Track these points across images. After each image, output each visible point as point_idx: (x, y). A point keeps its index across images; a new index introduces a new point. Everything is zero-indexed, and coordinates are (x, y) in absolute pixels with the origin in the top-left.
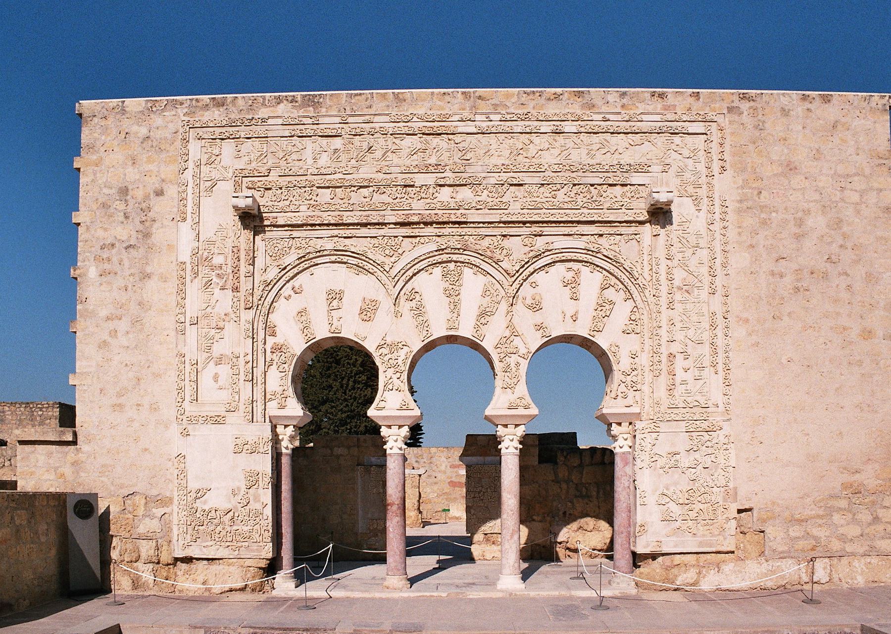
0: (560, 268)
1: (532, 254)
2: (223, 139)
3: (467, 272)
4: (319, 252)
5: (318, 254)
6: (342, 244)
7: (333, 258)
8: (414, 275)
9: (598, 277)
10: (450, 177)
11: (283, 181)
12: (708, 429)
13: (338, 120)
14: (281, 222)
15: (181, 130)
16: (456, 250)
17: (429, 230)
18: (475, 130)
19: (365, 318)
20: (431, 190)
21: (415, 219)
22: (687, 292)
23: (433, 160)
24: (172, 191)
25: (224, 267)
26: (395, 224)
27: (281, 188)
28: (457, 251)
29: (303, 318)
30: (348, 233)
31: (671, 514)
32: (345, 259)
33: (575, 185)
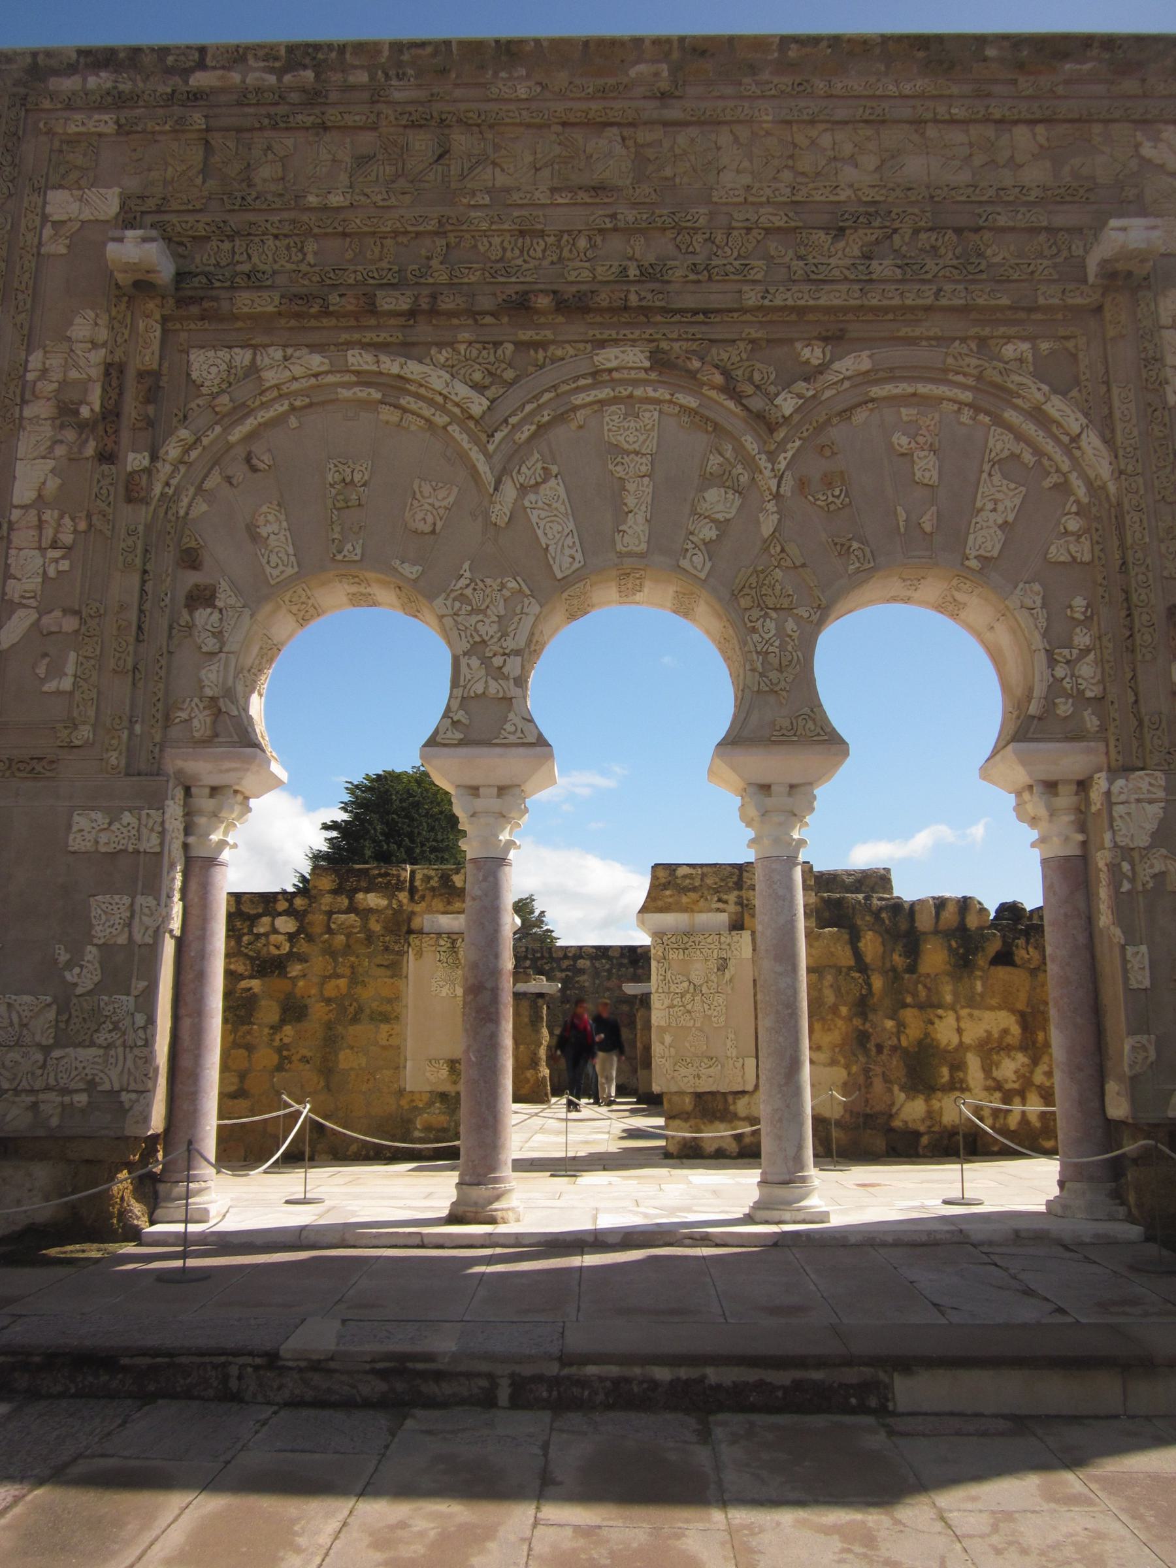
4: (316, 376)
10: (628, 215)
20: (582, 243)
27: (231, 238)
29: (269, 529)
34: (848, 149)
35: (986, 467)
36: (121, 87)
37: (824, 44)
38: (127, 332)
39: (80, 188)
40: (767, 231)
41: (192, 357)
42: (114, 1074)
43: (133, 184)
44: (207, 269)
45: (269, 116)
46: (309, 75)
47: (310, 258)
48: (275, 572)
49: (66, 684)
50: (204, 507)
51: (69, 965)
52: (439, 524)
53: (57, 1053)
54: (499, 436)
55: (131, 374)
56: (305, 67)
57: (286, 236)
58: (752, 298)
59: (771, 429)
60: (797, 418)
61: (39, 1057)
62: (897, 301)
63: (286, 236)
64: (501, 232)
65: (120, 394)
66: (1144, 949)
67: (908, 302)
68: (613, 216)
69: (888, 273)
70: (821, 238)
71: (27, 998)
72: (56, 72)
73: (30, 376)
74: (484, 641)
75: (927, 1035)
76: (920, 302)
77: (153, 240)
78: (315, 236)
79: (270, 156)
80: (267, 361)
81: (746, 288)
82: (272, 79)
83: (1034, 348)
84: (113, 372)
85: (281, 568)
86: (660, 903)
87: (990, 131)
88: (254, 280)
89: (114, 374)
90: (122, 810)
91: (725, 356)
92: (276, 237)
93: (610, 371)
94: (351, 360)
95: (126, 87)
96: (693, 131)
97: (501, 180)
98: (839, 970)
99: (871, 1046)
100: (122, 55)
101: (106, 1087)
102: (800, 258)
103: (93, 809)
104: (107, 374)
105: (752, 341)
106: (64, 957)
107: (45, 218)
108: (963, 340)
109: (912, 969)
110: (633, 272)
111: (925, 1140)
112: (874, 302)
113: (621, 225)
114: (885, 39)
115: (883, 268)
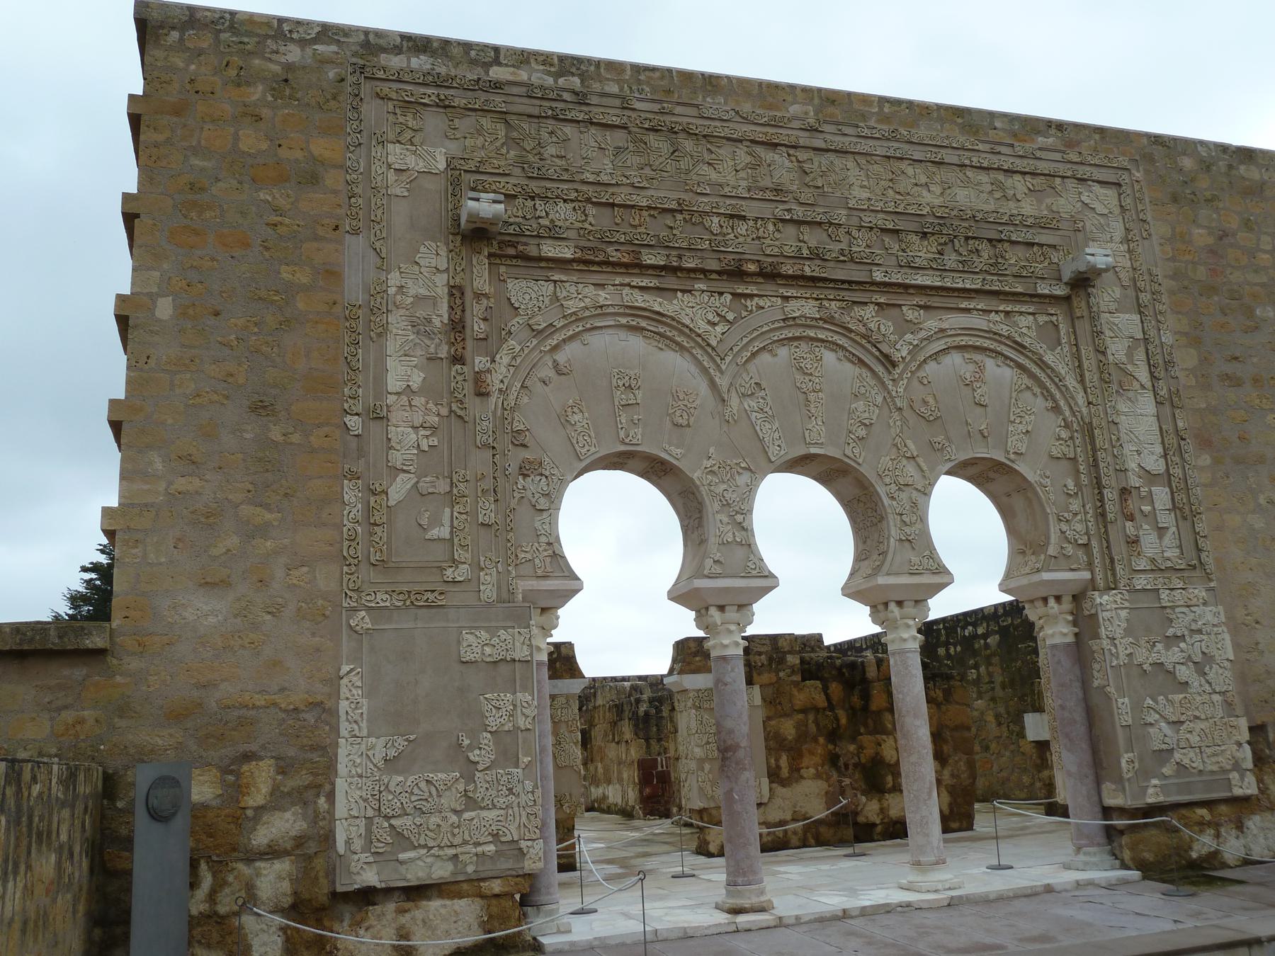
0: (956, 358)
1: (923, 334)
2: (425, 105)
3: (829, 357)
4: (601, 307)
5: (599, 311)
6: (639, 299)
7: (623, 321)
8: (754, 355)
9: (1007, 373)
10: (799, 212)
11: (534, 186)
12: (1190, 603)
13: (617, 102)
14: (533, 251)
15: (351, 79)
16: (811, 323)
17: (769, 288)
18: (823, 146)
19: (680, 421)
21: (752, 268)
22: (1130, 399)
23: (767, 182)
24: (332, 179)
25: (437, 322)
26: (719, 273)
27: (533, 198)
28: (813, 323)
29: (576, 417)
30: (645, 282)
31: (1167, 740)
32: (643, 324)
33: (967, 238)
34: (923, 179)
35: (1014, 394)
36: (438, 70)
37: (904, 106)
38: (464, 263)
39: (412, 144)
40: (882, 230)
41: (510, 286)
42: (513, 828)
43: (454, 148)
44: (517, 220)
45: (551, 108)
46: (577, 80)
47: (590, 219)
48: (584, 451)
49: (445, 532)
50: (526, 400)
51: (471, 748)
52: (692, 419)
53: (467, 815)
54: (728, 359)
55: (469, 295)
56: (573, 75)
57: (572, 201)
58: (878, 276)
59: (894, 365)
60: (908, 358)
61: (454, 818)
62: (960, 286)
63: (572, 201)
64: (719, 214)
65: (463, 311)
66: (1126, 700)
67: (968, 286)
68: (789, 210)
69: (954, 265)
70: (914, 238)
71: (441, 776)
72: (384, 50)
73: (392, 291)
74: (728, 504)
75: (877, 754)
76: (974, 287)
77: (500, 202)
78: (593, 203)
79: (554, 139)
80: (565, 293)
81: (875, 268)
82: (550, 81)
83: (1035, 319)
84: (456, 292)
85: (587, 447)
86: (693, 667)
87: (1001, 177)
88: (553, 233)
89: (457, 294)
90: (498, 628)
91: (862, 313)
92: (565, 201)
93: (794, 318)
94: (626, 298)
95: (443, 70)
96: (831, 156)
97: (714, 176)
98: (817, 710)
99: (841, 763)
100: (435, 45)
101: (509, 838)
102: (904, 251)
103: (477, 628)
104: (451, 295)
105: (877, 304)
106: (467, 742)
107: (389, 166)
108: (997, 312)
109: (865, 708)
110: (805, 252)
111: (879, 829)
112: (949, 285)
113: (795, 217)
114: (940, 107)
115: (951, 260)
